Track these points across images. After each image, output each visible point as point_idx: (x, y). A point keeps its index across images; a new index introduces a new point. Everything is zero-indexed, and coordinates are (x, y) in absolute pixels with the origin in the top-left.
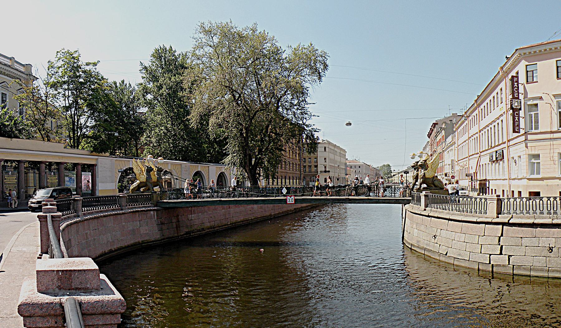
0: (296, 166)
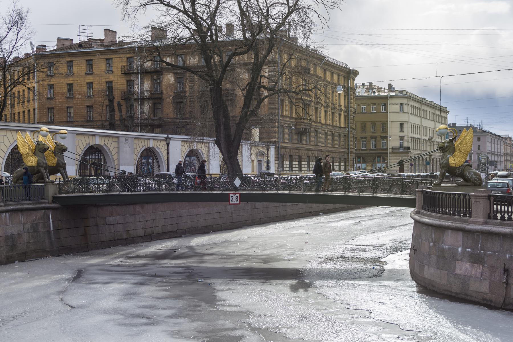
0: (340, 139)
